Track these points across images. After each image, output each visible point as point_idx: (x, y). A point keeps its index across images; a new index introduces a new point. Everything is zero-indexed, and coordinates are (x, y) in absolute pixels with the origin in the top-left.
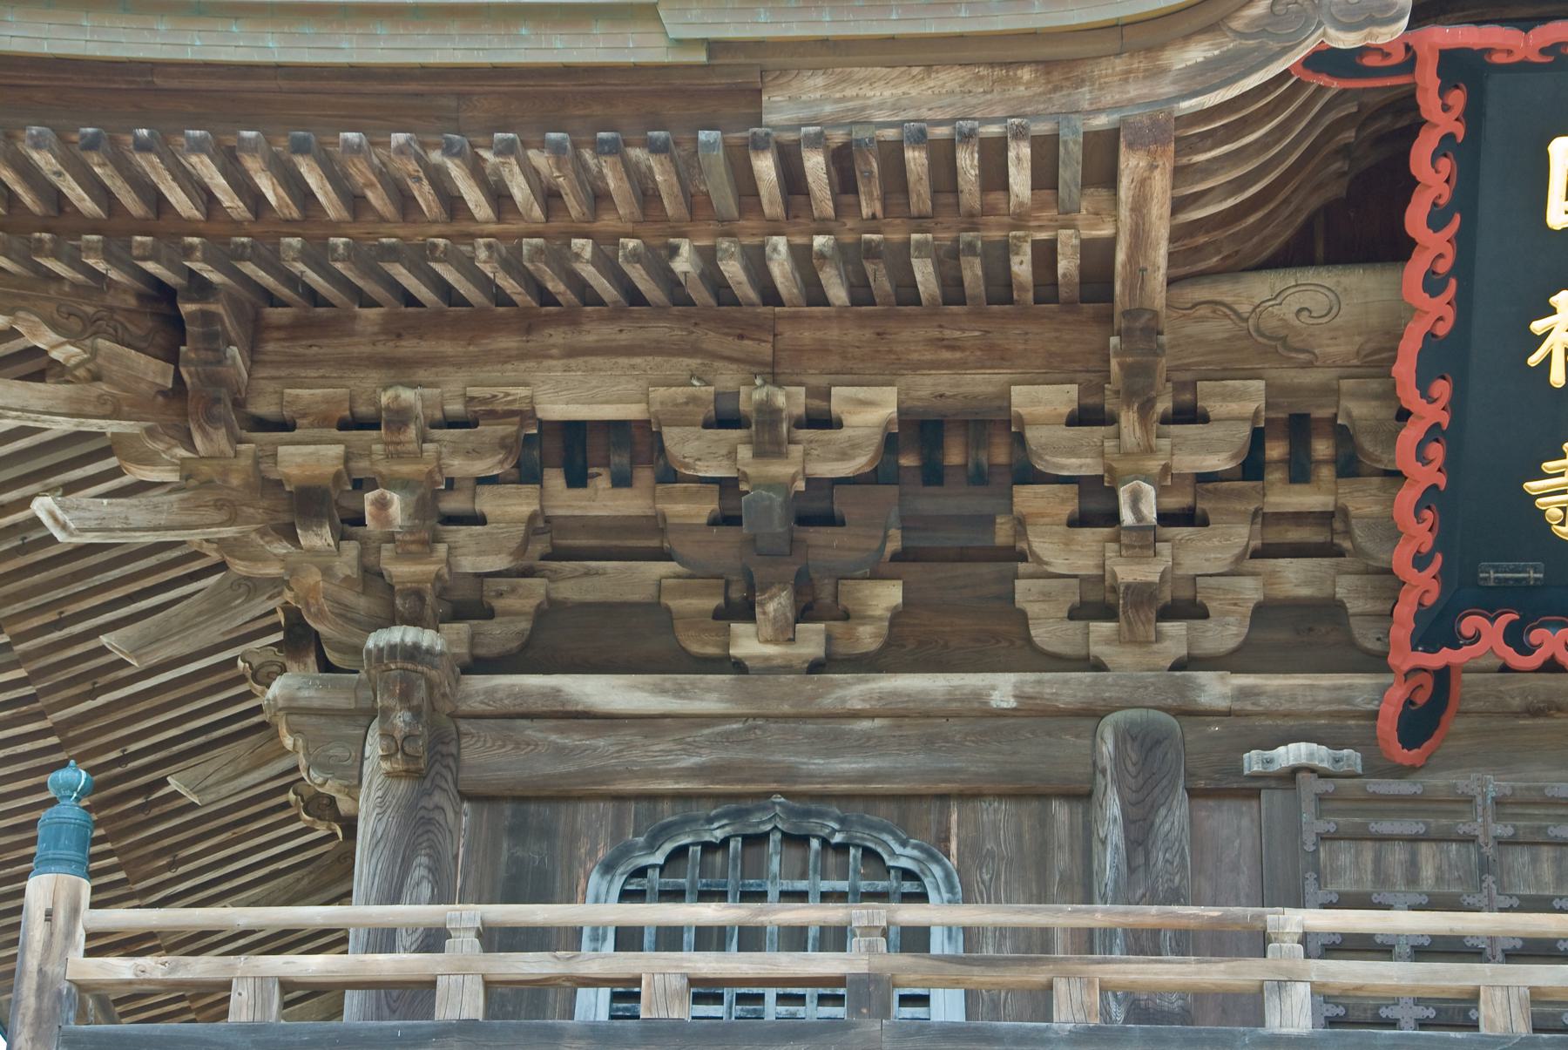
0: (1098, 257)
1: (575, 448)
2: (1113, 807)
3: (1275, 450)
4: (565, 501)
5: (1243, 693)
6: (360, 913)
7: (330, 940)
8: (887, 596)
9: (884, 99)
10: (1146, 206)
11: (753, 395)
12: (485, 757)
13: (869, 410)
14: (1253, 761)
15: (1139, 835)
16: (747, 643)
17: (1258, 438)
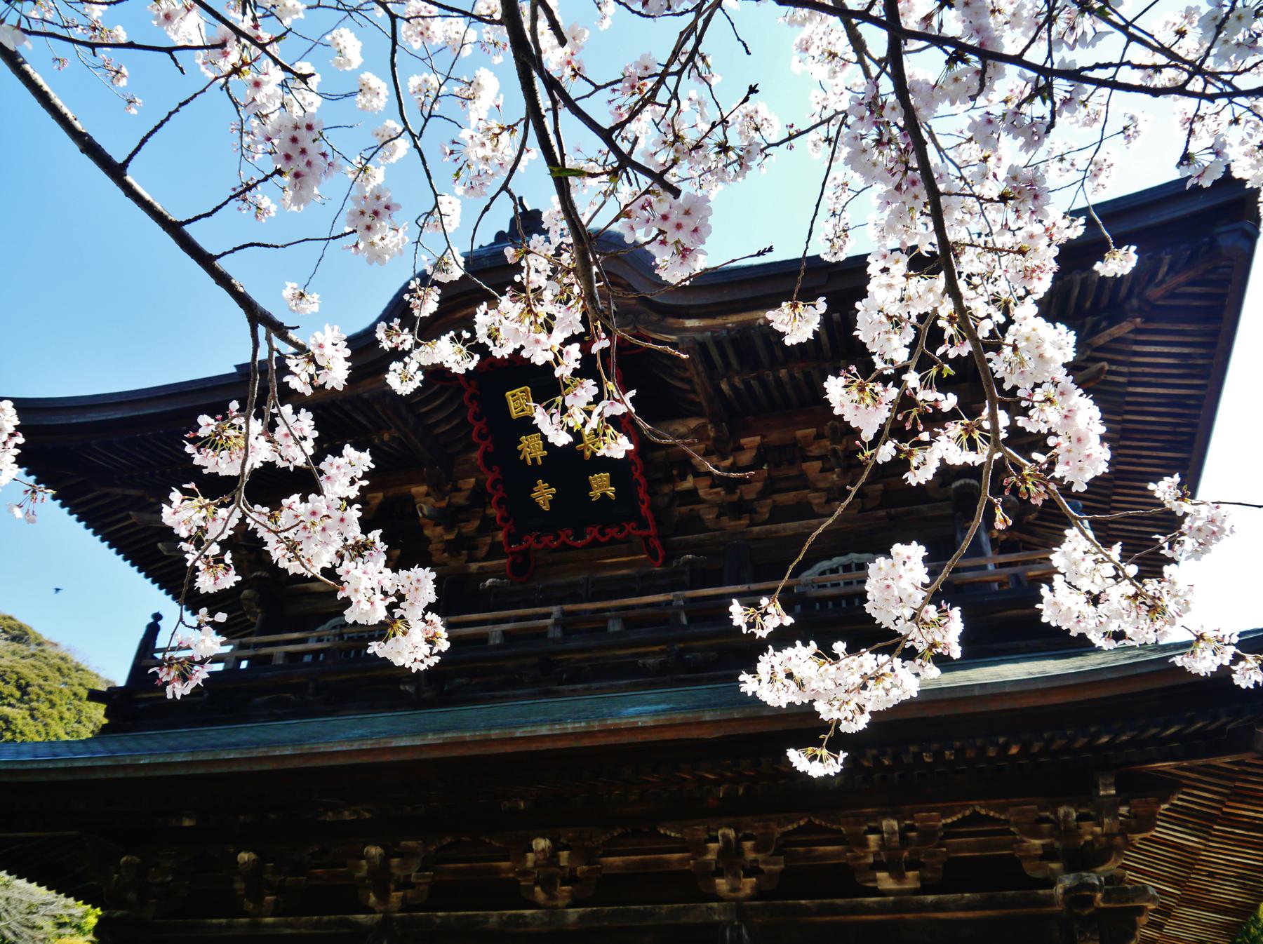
5: (481, 567)
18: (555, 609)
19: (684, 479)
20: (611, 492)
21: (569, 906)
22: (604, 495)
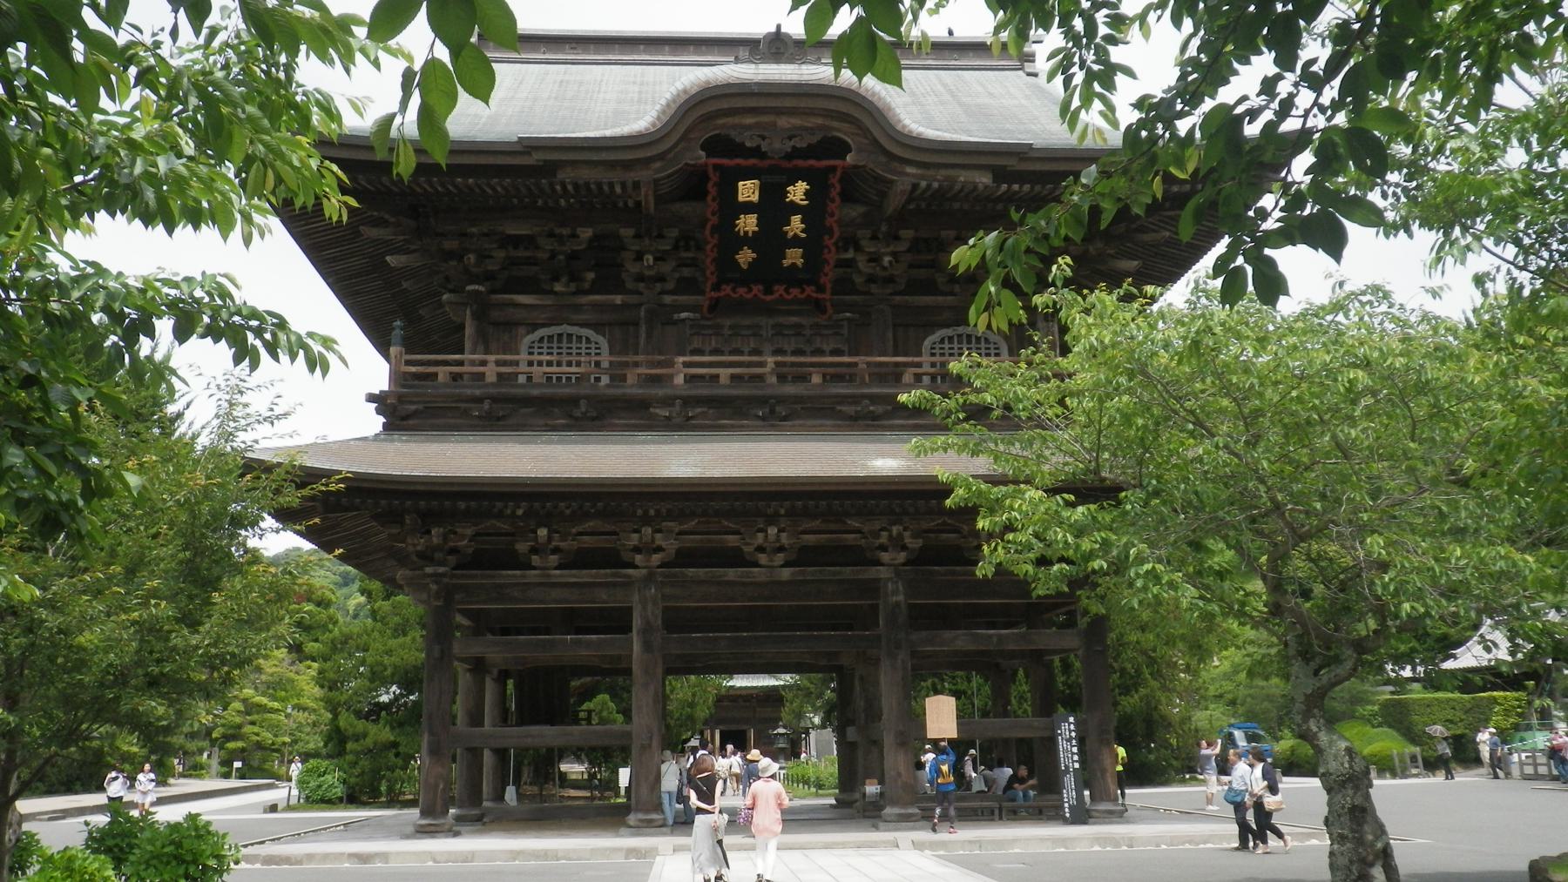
0: (638, 204)
1: (516, 241)
2: (643, 329)
3: (682, 244)
4: (514, 253)
6: (467, 356)
7: (461, 363)
9: (586, 174)
10: (647, 196)
11: (557, 231)
12: (495, 314)
13: (586, 233)
14: (676, 316)
15: (649, 336)
16: (558, 287)
19: (846, 250)
20: (800, 262)
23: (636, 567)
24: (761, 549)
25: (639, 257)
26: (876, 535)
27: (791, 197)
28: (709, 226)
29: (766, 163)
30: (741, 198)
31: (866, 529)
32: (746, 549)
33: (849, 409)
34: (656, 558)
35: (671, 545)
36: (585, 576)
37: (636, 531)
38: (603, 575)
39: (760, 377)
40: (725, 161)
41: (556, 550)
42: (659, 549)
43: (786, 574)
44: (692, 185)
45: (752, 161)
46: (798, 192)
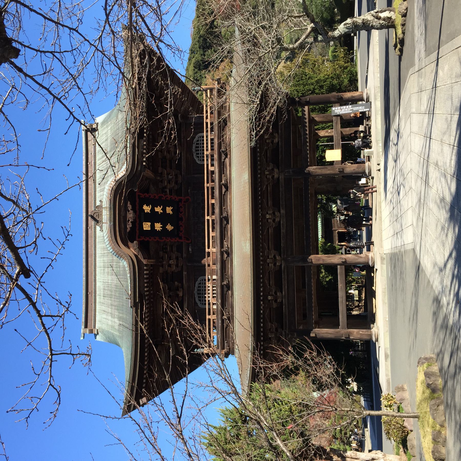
8: (176, 283)
16: (181, 294)
17: (164, 252)
18: (207, 218)
19: (166, 192)
21: (280, 213)
22: (172, 210)
23: (281, 264)
24: (274, 221)
25: (170, 265)
26: (268, 179)
27: (149, 211)
28: (159, 240)
29: (138, 220)
30: (149, 229)
31: (266, 183)
32: (274, 226)
33: (224, 190)
34: (278, 258)
35: (273, 252)
36: (285, 283)
37: (268, 265)
38: (284, 276)
39: (213, 221)
40: (137, 234)
41: (276, 293)
42: (275, 256)
43: (283, 211)
44: (144, 248)
45: (137, 225)
46: (147, 209)
